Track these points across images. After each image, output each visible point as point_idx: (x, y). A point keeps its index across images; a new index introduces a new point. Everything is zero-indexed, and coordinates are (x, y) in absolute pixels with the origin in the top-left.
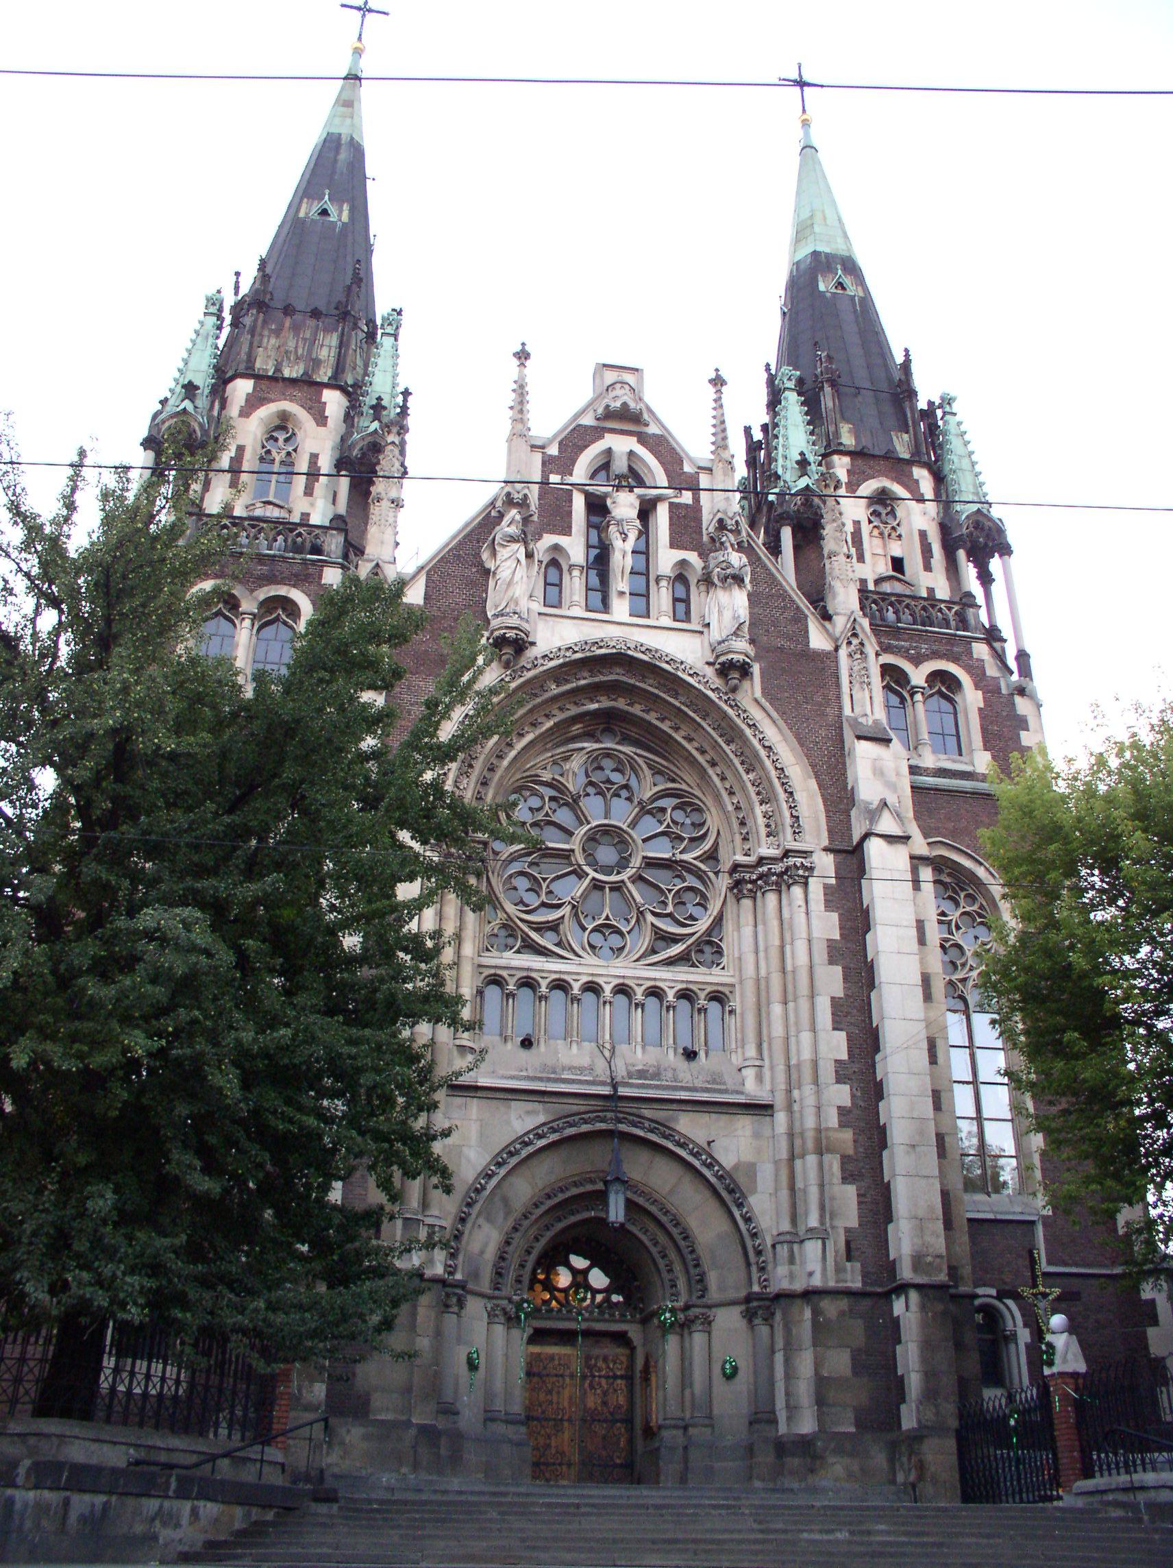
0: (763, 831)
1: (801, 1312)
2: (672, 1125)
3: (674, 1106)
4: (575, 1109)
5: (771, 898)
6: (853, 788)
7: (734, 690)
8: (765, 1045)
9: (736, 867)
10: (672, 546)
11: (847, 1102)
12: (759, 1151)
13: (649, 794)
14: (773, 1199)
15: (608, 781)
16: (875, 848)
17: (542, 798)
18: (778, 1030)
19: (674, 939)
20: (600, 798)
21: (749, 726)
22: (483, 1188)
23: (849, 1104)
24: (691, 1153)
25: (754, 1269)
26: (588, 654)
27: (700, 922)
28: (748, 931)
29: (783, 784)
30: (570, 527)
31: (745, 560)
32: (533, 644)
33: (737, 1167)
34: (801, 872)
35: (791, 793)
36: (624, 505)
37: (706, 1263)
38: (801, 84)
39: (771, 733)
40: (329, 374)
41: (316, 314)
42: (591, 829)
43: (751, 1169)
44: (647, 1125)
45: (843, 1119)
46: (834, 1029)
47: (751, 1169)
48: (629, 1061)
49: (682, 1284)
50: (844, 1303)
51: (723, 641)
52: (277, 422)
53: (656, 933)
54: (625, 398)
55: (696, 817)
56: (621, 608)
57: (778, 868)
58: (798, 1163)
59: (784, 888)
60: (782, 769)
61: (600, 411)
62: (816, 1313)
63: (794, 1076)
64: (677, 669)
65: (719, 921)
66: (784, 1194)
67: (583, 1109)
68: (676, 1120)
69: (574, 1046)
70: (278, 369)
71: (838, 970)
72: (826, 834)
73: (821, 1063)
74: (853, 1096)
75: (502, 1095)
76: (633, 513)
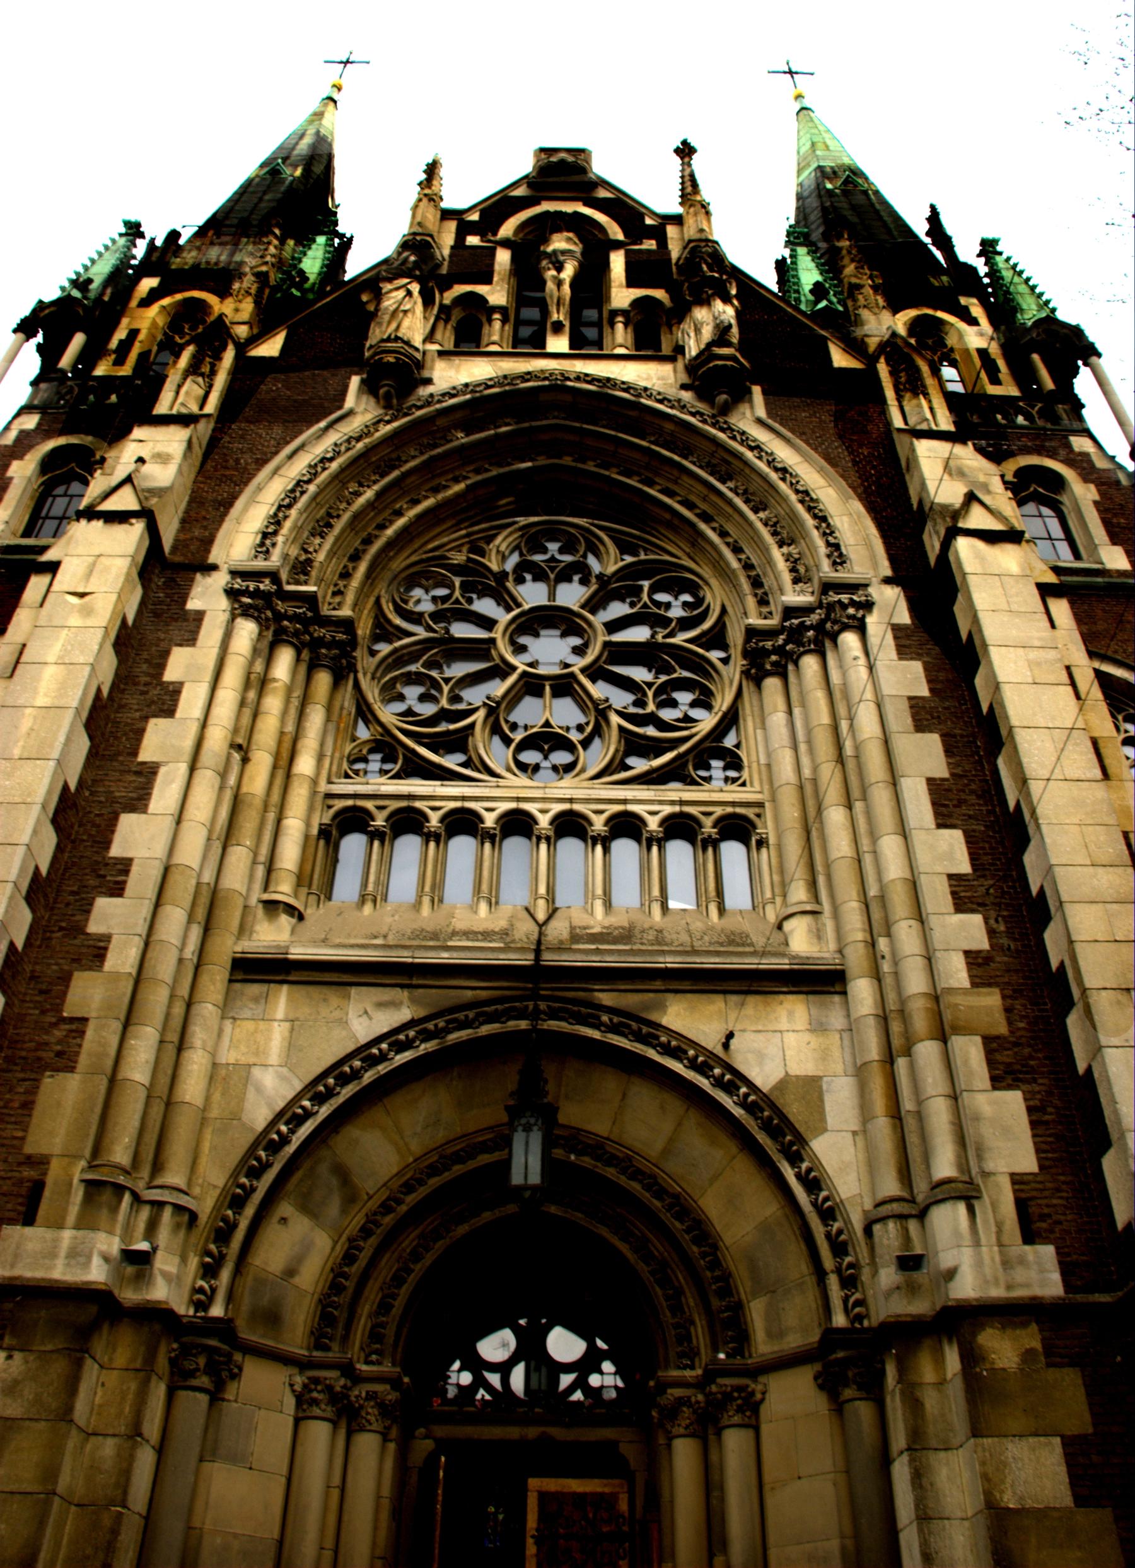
0: (787, 578)
1: (939, 1362)
2: (653, 1017)
3: (658, 985)
5: (810, 664)
6: (921, 502)
8: (821, 880)
9: (751, 633)
11: (982, 942)
12: (824, 1055)
14: (860, 1139)
15: (553, 559)
17: (451, 587)
18: (840, 845)
21: (751, 449)
22: (285, 1140)
24: (693, 1065)
25: (833, 1281)
26: (507, 388)
32: (429, 381)
33: (784, 1083)
34: (851, 611)
35: (824, 519)
37: (743, 1284)
39: (785, 454)
43: (812, 1087)
44: (605, 1018)
45: (978, 971)
46: (940, 826)
48: (577, 922)
49: (700, 1334)
50: (1030, 1337)
56: (558, 344)
57: (815, 618)
58: (901, 1063)
59: (828, 644)
62: (971, 1358)
63: (876, 915)
65: (731, 719)
66: (882, 1125)
67: (484, 994)
68: (662, 1007)
69: (483, 907)
71: (933, 742)
72: (886, 563)
73: (924, 880)
74: (991, 933)
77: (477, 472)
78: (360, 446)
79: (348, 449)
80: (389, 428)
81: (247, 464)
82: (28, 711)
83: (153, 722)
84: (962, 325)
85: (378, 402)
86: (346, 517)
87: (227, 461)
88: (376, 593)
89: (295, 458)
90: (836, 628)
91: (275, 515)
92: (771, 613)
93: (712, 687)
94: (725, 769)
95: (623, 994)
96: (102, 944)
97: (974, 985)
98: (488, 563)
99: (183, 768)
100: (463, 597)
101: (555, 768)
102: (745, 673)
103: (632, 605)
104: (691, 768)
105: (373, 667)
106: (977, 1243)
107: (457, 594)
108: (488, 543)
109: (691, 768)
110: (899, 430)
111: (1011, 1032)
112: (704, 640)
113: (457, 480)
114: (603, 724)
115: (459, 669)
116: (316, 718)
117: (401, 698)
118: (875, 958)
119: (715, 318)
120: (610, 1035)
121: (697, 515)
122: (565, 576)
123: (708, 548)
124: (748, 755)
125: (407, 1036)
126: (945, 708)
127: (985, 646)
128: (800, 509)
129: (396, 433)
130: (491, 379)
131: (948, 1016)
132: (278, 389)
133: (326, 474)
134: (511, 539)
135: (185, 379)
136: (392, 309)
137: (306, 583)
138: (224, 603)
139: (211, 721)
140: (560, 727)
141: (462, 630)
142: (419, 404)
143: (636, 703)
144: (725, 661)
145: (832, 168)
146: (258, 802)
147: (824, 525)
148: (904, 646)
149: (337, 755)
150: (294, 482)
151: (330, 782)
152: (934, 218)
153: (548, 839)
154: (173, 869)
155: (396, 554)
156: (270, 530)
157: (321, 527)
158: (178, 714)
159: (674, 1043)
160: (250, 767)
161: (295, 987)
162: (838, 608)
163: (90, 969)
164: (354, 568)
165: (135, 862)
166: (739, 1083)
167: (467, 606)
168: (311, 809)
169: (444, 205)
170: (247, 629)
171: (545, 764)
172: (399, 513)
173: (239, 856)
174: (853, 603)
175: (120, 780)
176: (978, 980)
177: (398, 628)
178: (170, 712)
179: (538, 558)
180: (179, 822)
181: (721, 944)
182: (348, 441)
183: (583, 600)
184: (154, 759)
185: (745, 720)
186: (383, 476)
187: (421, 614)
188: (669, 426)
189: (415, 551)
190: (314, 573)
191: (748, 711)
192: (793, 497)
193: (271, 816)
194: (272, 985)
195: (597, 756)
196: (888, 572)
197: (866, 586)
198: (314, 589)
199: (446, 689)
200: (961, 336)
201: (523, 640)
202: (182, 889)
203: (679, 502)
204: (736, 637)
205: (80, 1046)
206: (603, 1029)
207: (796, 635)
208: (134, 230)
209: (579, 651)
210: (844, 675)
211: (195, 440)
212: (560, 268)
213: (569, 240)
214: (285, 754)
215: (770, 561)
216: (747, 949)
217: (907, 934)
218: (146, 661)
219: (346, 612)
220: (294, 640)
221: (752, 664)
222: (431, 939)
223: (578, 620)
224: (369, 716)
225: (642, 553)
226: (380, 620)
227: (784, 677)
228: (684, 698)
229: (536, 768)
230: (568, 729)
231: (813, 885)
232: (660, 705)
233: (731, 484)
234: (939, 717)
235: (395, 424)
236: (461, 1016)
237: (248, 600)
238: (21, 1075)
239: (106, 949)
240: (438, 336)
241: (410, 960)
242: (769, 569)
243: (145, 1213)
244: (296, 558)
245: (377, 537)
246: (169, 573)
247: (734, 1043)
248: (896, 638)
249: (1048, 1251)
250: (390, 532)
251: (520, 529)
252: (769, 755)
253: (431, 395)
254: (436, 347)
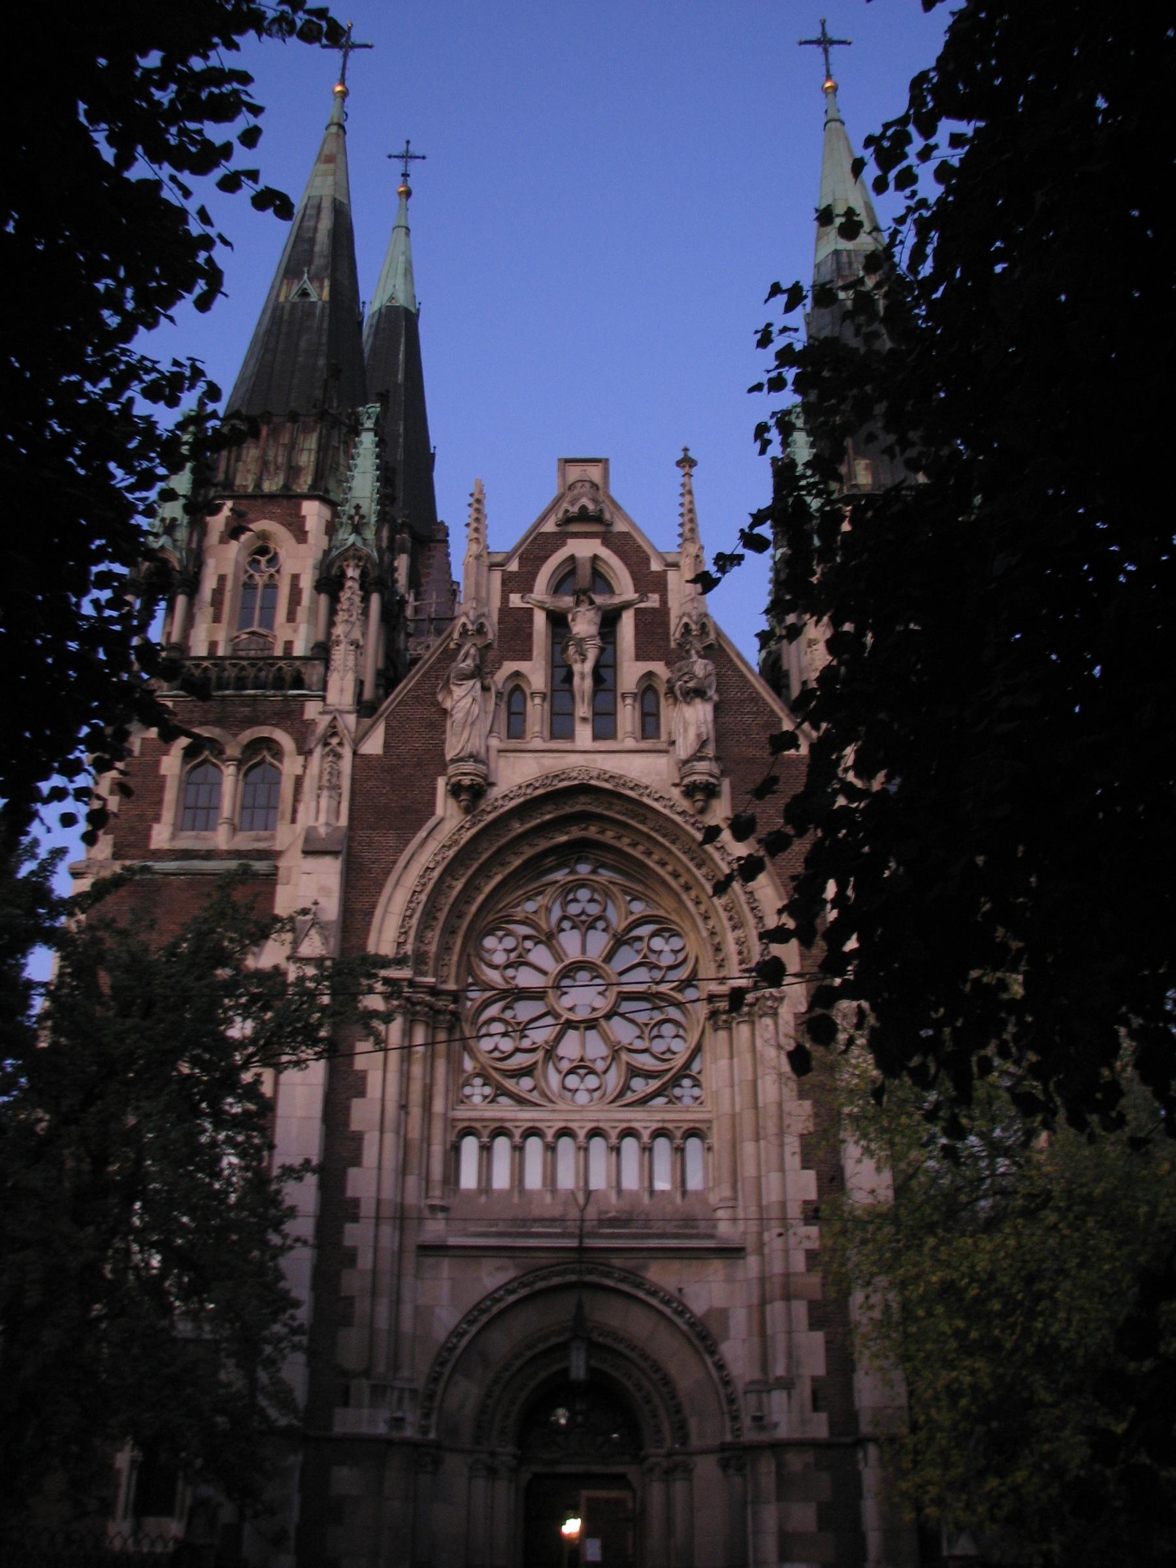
3: (645, 1254)
4: (544, 1262)
7: (702, 811)
8: (739, 1184)
10: (638, 657)
13: (624, 925)
18: (748, 1169)
20: (575, 931)
22: (455, 1347)
25: (727, 1418)
26: (550, 789)
27: (677, 1056)
28: (724, 1063)
29: (753, 909)
30: (531, 651)
31: (710, 667)
32: (492, 784)
33: (710, 1312)
35: (761, 918)
36: (584, 625)
40: (309, 482)
41: (294, 417)
42: (565, 967)
43: (722, 1315)
46: (804, 1168)
47: (722, 1315)
50: (809, 1456)
53: (632, 1071)
54: (584, 501)
55: (676, 943)
56: (584, 734)
58: (768, 1307)
60: (751, 893)
61: (560, 515)
62: (780, 1465)
64: (641, 795)
65: (697, 1050)
66: (756, 1340)
70: (258, 485)
75: (473, 1253)
76: (593, 630)
99: (377, 1134)
106: (790, 1411)
115: (525, 1010)
141: (526, 978)
168: (445, 1130)
173: (412, 1181)
227: (730, 1029)
228: (668, 1030)
243: (396, 1394)
247: (685, 1291)
249: (823, 1416)
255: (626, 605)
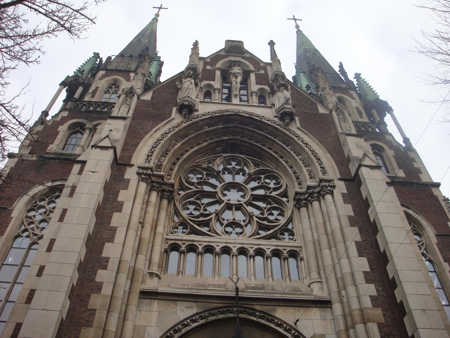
0: (308, 177)
2: (273, 314)
3: (273, 303)
5: (316, 204)
6: (348, 156)
7: (288, 124)
8: (322, 272)
9: (297, 193)
11: (375, 293)
15: (234, 167)
16: (364, 171)
17: (202, 174)
18: (328, 261)
19: (267, 228)
21: (296, 137)
23: (376, 294)
24: (286, 330)
26: (221, 114)
32: (197, 110)
34: (329, 188)
35: (319, 159)
38: (295, 19)
39: (306, 139)
44: (258, 314)
46: (359, 256)
51: (281, 106)
52: (113, 82)
53: (259, 226)
57: (317, 190)
58: (351, 331)
59: (321, 198)
63: (341, 283)
65: (290, 220)
67: (220, 305)
68: (275, 311)
71: (356, 229)
72: (339, 174)
74: (377, 290)
77: (211, 139)
78: (177, 129)
79: (173, 130)
80: (185, 124)
81: (142, 133)
82: (78, 209)
83: (115, 213)
84: (350, 99)
85: (182, 116)
86: (172, 151)
87: (135, 132)
88: (180, 176)
89: (157, 132)
90: (324, 193)
91: (151, 150)
92: (302, 187)
93: (284, 210)
94: (289, 235)
95: (263, 306)
96: (100, 285)
97: (373, 306)
98: (214, 168)
99: (125, 229)
100: (207, 178)
101: (237, 233)
102: (295, 206)
103: (259, 183)
104: (279, 235)
105: (179, 199)
107: (205, 177)
108: (214, 161)
109: (279, 235)
110: (340, 133)
111: (386, 322)
112: (281, 195)
113: (205, 141)
114: (251, 220)
115: (205, 201)
116: (163, 214)
117: (188, 209)
118: (341, 297)
119: (284, 96)
120: (259, 319)
121: (279, 156)
122: (238, 173)
123: (282, 166)
124: (296, 231)
125: (196, 318)
126: (359, 220)
127: (372, 201)
128: (312, 156)
129: (188, 126)
130: (216, 111)
131: (366, 316)
132: (150, 110)
133: (167, 137)
134: (221, 160)
135: (122, 105)
136: (186, 87)
137: (160, 172)
138: (136, 177)
139: (133, 214)
140: (239, 221)
141: (207, 188)
142: (194, 117)
143: (261, 214)
144: (288, 202)
145: (309, 49)
146: (147, 241)
147: (319, 161)
148: (345, 200)
149: (169, 226)
150: (157, 140)
151: (167, 235)
152: (341, 66)
153: (236, 256)
154: (122, 261)
155: (186, 163)
156: (150, 154)
157: (165, 154)
158: (123, 212)
159: (279, 322)
160: (144, 229)
161: (159, 301)
162: (325, 187)
163: (97, 293)
164: (174, 167)
165: (110, 259)
166: (300, 336)
167: (208, 181)
168: (162, 243)
169: (200, 56)
170: (143, 186)
171: (233, 232)
172: (187, 151)
173: (141, 258)
174: (329, 186)
175: (104, 232)
176: (375, 305)
177: (187, 187)
178: (120, 211)
179: (229, 167)
180: (123, 246)
181: (292, 291)
182: (173, 127)
183: (244, 181)
184: (116, 226)
185: (295, 220)
186: (183, 139)
187: (194, 183)
188: (270, 128)
189: (191, 163)
190: (163, 169)
191: (296, 217)
192: (310, 152)
193: (151, 245)
194: (152, 300)
195: (249, 230)
196: (340, 177)
197: (333, 181)
198: (163, 174)
199: (202, 207)
200: (350, 103)
201: (225, 192)
202: (125, 268)
203: (273, 152)
204: (291, 194)
205: (94, 319)
206: (257, 317)
207: (311, 195)
208: (97, 55)
209: (243, 197)
210: (327, 208)
211: (126, 125)
212: (236, 77)
213: (239, 69)
214: (154, 226)
215: (302, 171)
216: (300, 293)
217: (351, 290)
218: (112, 194)
219: (172, 181)
220: (157, 189)
221: (297, 203)
222: (202, 287)
223: (242, 187)
224: (179, 214)
225: (261, 167)
226: (181, 184)
227: (307, 208)
228: (276, 213)
229: (231, 233)
230: (240, 221)
231: (319, 273)
232: (269, 214)
233: (290, 147)
234: (357, 222)
235: (187, 123)
236: (213, 312)
237: (144, 176)
238: (74, 328)
239: (102, 287)
240: (199, 96)
241: (196, 293)
242: (301, 174)
244: (157, 164)
245: (181, 158)
246: (118, 166)
247: (298, 323)
248: (343, 197)
250: (185, 156)
251: (224, 157)
252: (303, 232)
253: (198, 115)
254: (199, 100)
255: (252, 71)
